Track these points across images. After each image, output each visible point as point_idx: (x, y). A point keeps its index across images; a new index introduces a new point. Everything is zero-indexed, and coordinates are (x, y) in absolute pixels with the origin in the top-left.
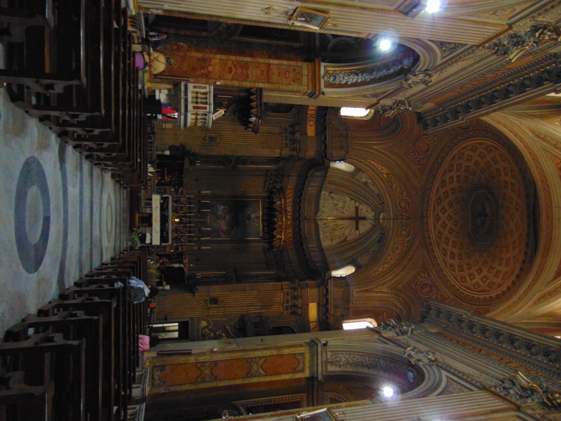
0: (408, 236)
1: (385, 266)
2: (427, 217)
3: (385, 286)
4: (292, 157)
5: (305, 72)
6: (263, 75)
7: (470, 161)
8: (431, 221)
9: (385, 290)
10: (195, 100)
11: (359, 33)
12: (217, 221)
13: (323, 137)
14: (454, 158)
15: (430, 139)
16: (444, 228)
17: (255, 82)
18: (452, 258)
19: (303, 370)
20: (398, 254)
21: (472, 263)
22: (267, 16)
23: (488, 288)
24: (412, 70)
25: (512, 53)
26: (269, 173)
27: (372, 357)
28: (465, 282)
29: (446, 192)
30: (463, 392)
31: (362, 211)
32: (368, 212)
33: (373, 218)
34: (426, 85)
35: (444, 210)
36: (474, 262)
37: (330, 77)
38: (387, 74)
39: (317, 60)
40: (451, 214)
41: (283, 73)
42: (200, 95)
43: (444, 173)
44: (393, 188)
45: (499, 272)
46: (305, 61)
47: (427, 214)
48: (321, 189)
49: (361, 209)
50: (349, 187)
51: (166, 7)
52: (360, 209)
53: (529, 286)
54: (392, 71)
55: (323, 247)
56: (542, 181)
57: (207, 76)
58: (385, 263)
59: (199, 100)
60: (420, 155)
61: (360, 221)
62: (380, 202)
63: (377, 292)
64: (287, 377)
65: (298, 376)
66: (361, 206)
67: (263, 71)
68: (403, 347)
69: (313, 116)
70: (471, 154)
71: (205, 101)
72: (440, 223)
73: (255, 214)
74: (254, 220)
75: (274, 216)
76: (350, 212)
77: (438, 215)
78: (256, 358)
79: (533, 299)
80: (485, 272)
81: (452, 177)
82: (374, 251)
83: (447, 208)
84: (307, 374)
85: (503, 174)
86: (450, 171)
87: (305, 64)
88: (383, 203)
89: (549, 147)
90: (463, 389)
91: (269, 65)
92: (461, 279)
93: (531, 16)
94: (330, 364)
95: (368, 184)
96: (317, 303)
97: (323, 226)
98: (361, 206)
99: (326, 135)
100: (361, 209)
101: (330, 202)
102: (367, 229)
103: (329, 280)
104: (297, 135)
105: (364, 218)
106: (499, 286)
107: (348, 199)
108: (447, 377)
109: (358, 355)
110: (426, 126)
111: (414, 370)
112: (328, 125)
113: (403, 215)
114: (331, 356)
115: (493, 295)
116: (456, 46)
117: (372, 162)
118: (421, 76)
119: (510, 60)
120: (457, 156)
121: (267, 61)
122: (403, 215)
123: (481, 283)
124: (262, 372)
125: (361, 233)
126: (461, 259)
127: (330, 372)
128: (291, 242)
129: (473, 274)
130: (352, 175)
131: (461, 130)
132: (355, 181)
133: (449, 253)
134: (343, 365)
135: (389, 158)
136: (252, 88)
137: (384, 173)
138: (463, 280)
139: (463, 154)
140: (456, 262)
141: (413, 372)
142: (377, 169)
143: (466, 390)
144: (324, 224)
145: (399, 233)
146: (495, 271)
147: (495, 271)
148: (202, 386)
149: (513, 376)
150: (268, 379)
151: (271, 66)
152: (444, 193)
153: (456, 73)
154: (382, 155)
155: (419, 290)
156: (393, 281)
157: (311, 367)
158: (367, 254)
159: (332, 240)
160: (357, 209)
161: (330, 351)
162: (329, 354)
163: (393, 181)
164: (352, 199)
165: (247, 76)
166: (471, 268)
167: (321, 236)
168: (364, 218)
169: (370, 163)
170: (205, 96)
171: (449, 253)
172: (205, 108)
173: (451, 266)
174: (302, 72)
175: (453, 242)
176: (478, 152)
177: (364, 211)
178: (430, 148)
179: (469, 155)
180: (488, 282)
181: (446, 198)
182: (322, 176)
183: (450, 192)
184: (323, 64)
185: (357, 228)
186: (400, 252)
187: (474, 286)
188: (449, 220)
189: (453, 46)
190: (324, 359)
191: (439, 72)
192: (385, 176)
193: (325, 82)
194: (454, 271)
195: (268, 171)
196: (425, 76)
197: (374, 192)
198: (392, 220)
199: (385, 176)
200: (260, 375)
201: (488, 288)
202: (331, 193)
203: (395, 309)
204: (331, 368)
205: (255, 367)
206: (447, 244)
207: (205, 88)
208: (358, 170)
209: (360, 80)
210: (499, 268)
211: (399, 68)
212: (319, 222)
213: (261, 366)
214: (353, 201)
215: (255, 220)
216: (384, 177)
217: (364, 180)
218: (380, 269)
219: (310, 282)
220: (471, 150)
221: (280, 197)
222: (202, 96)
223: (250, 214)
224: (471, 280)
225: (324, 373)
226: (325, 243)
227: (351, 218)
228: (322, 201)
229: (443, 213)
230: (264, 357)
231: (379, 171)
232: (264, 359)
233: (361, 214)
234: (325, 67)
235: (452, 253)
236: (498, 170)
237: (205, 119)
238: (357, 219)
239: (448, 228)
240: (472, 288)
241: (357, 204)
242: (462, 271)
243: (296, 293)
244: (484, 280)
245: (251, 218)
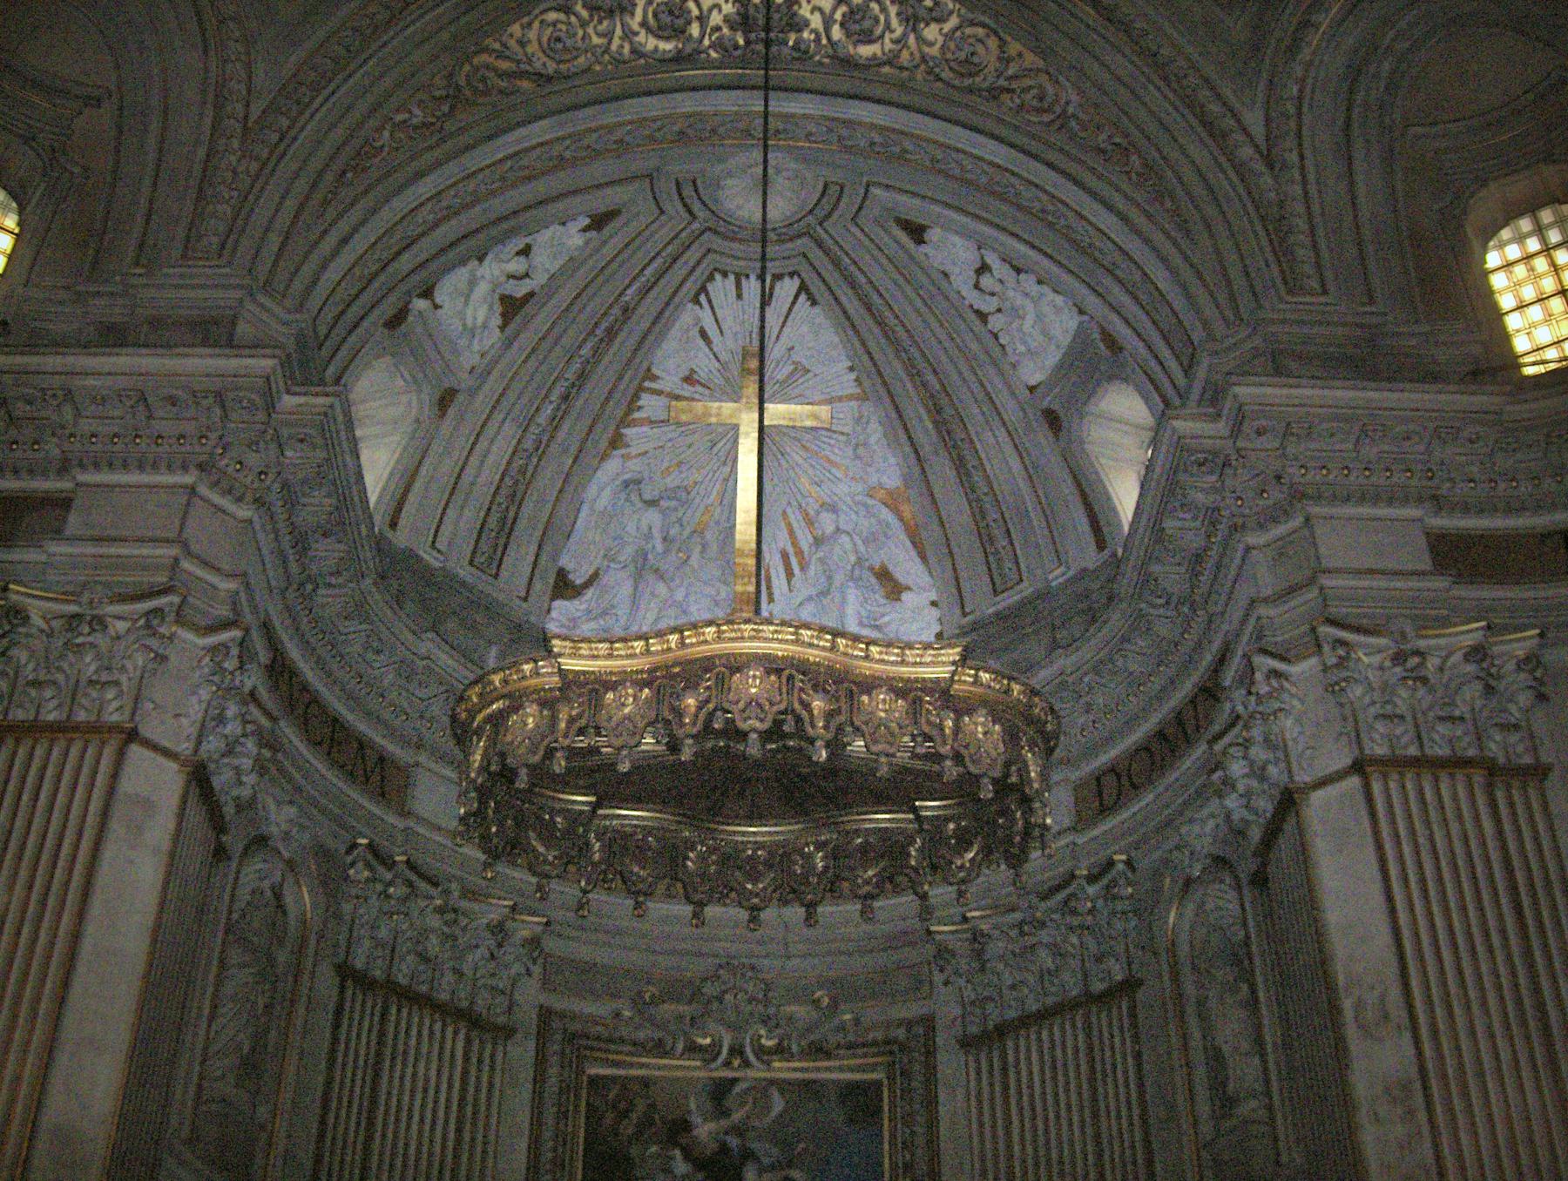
31: (702, 375)
32: (712, 332)
33: (752, 287)
44: (551, 67)
50: (528, 444)
73: (696, 1119)
74: (739, 1131)
95: (520, 290)
132: (493, 385)
145: (866, 51)
158: (996, 322)
159: (893, 587)
163: (505, 65)
186: (993, 43)
197: (573, 264)
198: (783, 105)
214: (629, 432)
215: (737, 1116)
217: (481, 311)
223: (687, 1156)
245: (724, 1149)
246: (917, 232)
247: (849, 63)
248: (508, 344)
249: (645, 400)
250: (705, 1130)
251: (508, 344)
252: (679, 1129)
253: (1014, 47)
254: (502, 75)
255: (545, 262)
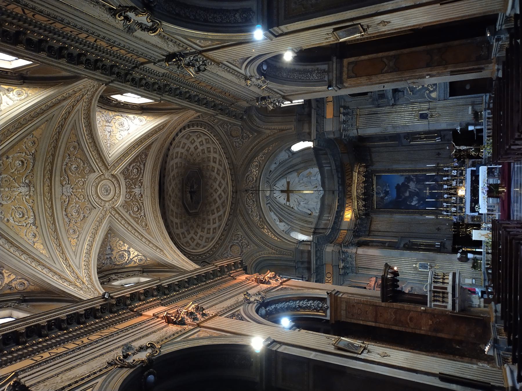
0: (247, 176)
1: (266, 151)
2: (233, 192)
3: (267, 135)
4: (347, 246)
5: (343, 313)
6: (381, 313)
7: (201, 236)
8: (230, 188)
9: (268, 132)
10: (445, 295)
11: (306, 332)
12: (417, 190)
13: (318, 263)
14: (213, 238)
15: (230, 256)
16: (220, 182)
17: (388, 307)
18: (214, 158)
19: (349, 64)
20: (256, 162)
21: (201, 154)
22: (385, 351)
23: (191, 134)
24: (259, 305)
25: (193, 308)
26: (367, 233)
27: (292, 79)
28: (206, 139)
29: (218, 212)
30: (233, 60)
33: (275, 192)
34: (248, 293)
35: (220, 196)
36: (200, 155)
37: (322, 307)
38: (277, 305)
39: (333, 322)
40: (214, 193)
41: (363, 313)
42: (441, 299)
43: (219, 227)
45: (183, 148)
46: (344, 322)
47: (233, 194)
48: (320, 217)
49: (285, 199)
51: (475, 367)
52: (286, 200)
53: (169, 137)
54: (273, 307)
55: (317, 167)
56: (157, 216)
57: (432, 314)
58: (266, 154)
59: (441, 295)
60: (237, 243)
61: (286, 189)
62: (269, 205)
63: (274, 129)
64: (363, 57)
65: (353, 59)
66: (284, 202)
67: (381, 316)
68: (268, 88)
69: (327, 281)
70: (199, 242)
71: (436, 294)
72: (223, 187)
74: (382, 192)
75: (364, 194)
76: (293, 197)
77: (225, 194)
78: (391, 72)
79: (167, 128)
80: (192, 147)
81: (214, 223)
82: (275, 163)
83: (218, 199)
84: (346, 61)
85: (179, 224)
86: (215, 229)
87: (342, 320)
88: (267, 204)
89: (153, 241)
90: (232, 62)
91: (376, 322)
92: (209, 142)
93: (185, 331)
94: (326, 70)
96: (326, 118)
97: (317, 185)
98: (284, 202)
99: (316, 264)
100: (284, 199)
101: (311, 207)
102: (280, 182)
103: (315, 138)
104: (342, 265)
105: (282, 191)
106: (183, 137)
107: (295, 208)
108: (241, 69)
109: (303, 79)
110: (241, 263)
111: (263, 71)
112: (314, 273)
113: (251, 193)
114: (324, 77)
115: (187, 129)
116: (232, 316)
117: (276, 239)
118: (252, 299)
119: (193, 303)
120: (210, 240)
121: (377, 325)
122: (251, 193)
123: (195, 139)
124: (385, 60)
125: (285, 179)
126: (208, 157)
127: (326, 64)
128: (347, 171)
129: (201, 145)
130: (292, 229)
131: (207, 261)
133: (217, 162)
134: (315, 70)
135: (262, 241)
136: (390, 302)
137: (267, 229)
138: (207, 141)
139: (206, 242)
140: (212, 155)
141: (263, 70)
142: (272, 233)
143: (230, 61)
144: (317, 187)
146: (186, 148)
147: (186, 148)
148: (440, 45)
149: (198, 74)
150: (380, 55)
151: (373, 320)
152: (220, 211)
153: (226, 299)
154: (268, 244)
155: (241, 132)
156: (261, 139)
157: (342, 66)
160: (288, 200)
161: (326, 81)
162: (326, 79)
164: (292, 208)
165: (395, 313)
166: (202, 150)
167: (319, 177)
168: (282, 191)
169: (278, 238)
170: (435, 298)
171: (217, 162)
172: (435, 287)
173: (216, 152)
174: (346, 313)
175: (214, 171)
176: (195, 242)
177: (282, 198)
178: (230, 249)
179: (202, 241)
180: (191, 139)
181: (218, 207)
182: (317, 229)
183: (215, 211)
184: (328, 318)
185: (288, 183)
187: (200, 136)
188: (216, 189)
189: (234, 318)
190: (330, 74)
191: (239, 301)
192: (265, 227)
193: (326, 303)
194: (214, 148)
195: (369, 235)
196: (249, 299)
197: (275, 213)
199: (265, 227)
200: (387, 57)
201: (191, 134)
202: (310, 214)
203: (260, 115)
204: (325, 67)
205: (391, 64)
206: (218, 170)
207: (435, 305)
208: (288, 233)
209: (297, 302)
210: (183, 151)
211: (268, 308)
212: (321, 189)
213: (386, 65)
216: (266, 226)
218: (271, 148)
219: (331, 136)
220: (200, 245)
221: (359, 210)
222: (437, 298)
224: (202, 141)
225: (331, 62)
226: (315, 170)
227: (292, 191)
228: (319, 206)
229: (220, 194)
230: (383, 73)
231: (271, 231)
232: (383, 72)
233: (285, 195)
234: (326, 316)
235: (215, 162)
236: (182, 227)
237: (435, 278)
238: (288, 192)
239: (218, 182)
240: (202, 135)
241: (288, 204)
242: (208, 148)
243: (345, 126)
244: (193, 141)
246: (271, 171)
247: (256, 181)
248: (284, 222)
249: (287, 205)
250: (382, 195)
251: (284, 222)
252: (382, 198)
253: (255, 161)
254: (260, 222)
255: (275, 217)
